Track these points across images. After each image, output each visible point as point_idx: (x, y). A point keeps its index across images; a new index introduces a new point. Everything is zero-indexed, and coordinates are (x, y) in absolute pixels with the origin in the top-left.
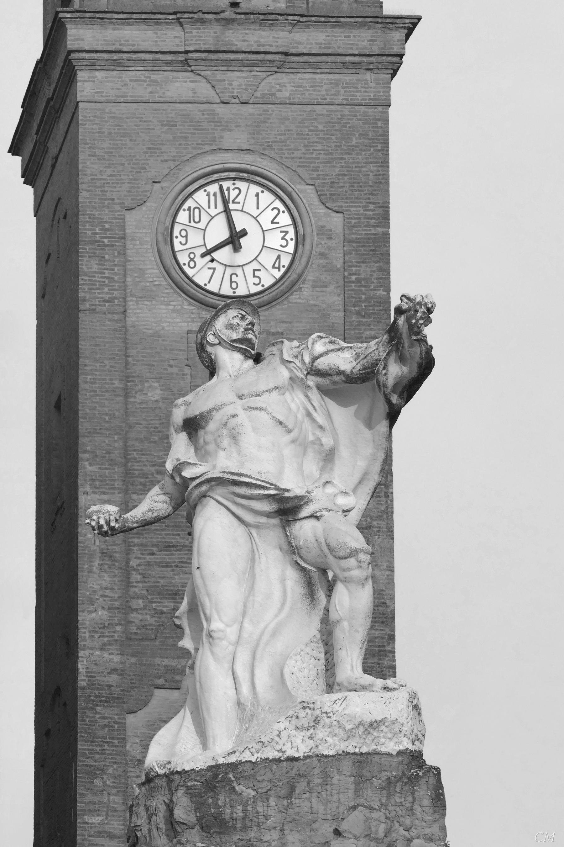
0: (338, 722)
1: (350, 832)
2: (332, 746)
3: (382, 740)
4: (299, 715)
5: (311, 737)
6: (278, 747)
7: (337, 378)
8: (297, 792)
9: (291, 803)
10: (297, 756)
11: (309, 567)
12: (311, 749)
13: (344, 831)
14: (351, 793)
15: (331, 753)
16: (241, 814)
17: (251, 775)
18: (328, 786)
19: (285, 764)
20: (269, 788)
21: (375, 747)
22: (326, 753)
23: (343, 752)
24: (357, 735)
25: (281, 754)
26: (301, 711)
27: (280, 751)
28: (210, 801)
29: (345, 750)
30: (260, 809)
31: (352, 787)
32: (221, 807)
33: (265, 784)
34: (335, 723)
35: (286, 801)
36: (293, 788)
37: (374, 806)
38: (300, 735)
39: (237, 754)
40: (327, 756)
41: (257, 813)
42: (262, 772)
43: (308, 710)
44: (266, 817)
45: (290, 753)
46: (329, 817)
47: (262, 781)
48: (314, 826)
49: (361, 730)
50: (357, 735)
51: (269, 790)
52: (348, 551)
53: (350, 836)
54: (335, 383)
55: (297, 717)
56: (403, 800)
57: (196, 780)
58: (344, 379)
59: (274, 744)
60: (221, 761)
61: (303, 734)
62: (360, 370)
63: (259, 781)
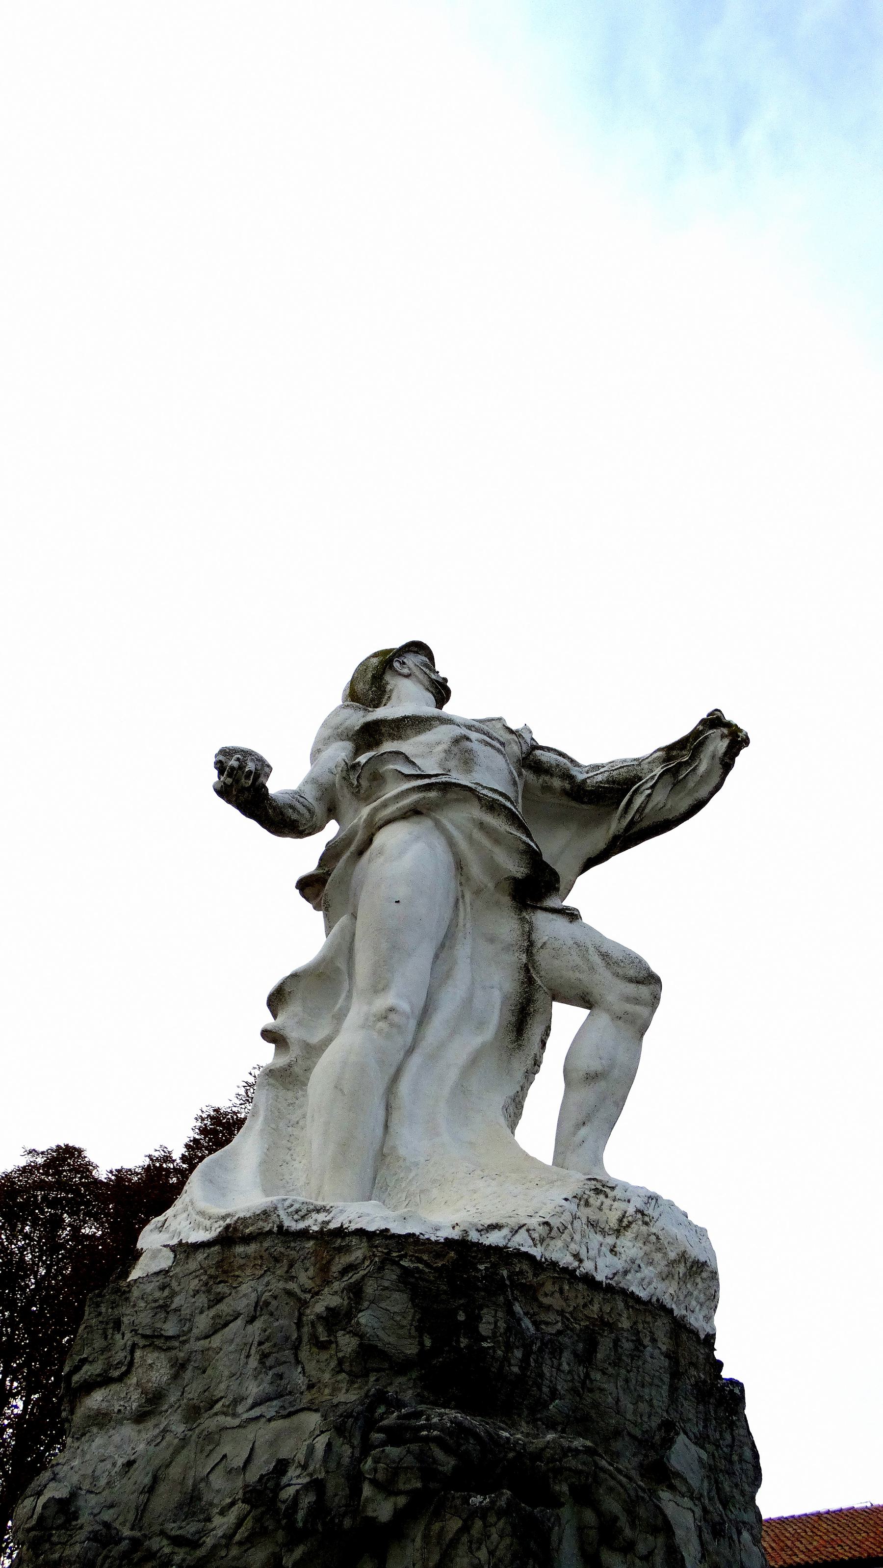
0: (658, 1238)
1: (685, 1480)
2: (646, 1281)
3: (694, 1303)
4: (591, 1200)
5: (613, 1250)
6: (574, 1247)
7: (557, 783)
8: (599, 1356)
9: (587, 1375)
10: (600, 1277)
11: (539, 982)
12: (615, 1274)
13: (677, 1475)
14: (665, 1390)
15: (643, 1294)
16: (515, 1369)
17: (531, 1286)
18: (640, 1363)
19: (580, 1286)
20: (559, 1326)
21: (684, 1312)
22: (634, 1289)
23: (658, 1300)
24: (676, 1277)
25: (576, 1264)
26: (592, 1194)
27: (576, 1256)
28: (461, 1317)
29: (661, 1298)
30: (546, 1370)
31: (666, 1378)
32: (485, 1339)
33: (551, 1317)
34: (653, 1238)
35: (581, 1368)
36: (592, 1346)
37: (690, 1434)
38: (596, 1239)
39: (505, 1231)
40: (638, 1299)
41: (541, 1375)
42: (549, 1287)
43: (602, 1197)
44: (554, 1394)
45: (588, 1266)
46: (637, 1432)
47: (549, 1308)
48: (617, 1445)
49: (682, 1269)
50: (676, 1277)
51: (559, 1333)
52: (643, 973)
53: (684, 1489)
54: (546, 788)
55: (587, 1204)
56: (718, 1436)
57: (420, 1260)
58: (568, 786)
59: (566, 1236)
60: (474, 1236)
61: (599, 1237)
62: (601, 782)
63: (541, 1305)
